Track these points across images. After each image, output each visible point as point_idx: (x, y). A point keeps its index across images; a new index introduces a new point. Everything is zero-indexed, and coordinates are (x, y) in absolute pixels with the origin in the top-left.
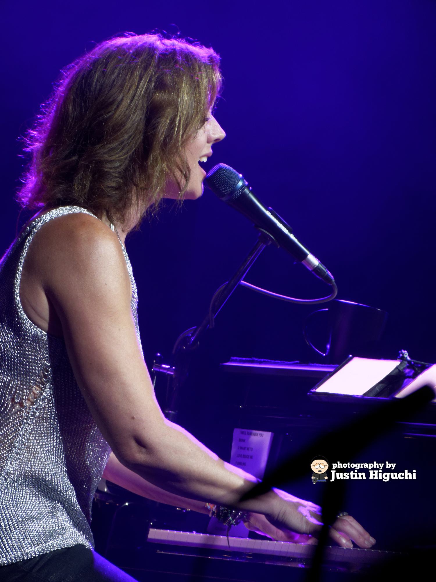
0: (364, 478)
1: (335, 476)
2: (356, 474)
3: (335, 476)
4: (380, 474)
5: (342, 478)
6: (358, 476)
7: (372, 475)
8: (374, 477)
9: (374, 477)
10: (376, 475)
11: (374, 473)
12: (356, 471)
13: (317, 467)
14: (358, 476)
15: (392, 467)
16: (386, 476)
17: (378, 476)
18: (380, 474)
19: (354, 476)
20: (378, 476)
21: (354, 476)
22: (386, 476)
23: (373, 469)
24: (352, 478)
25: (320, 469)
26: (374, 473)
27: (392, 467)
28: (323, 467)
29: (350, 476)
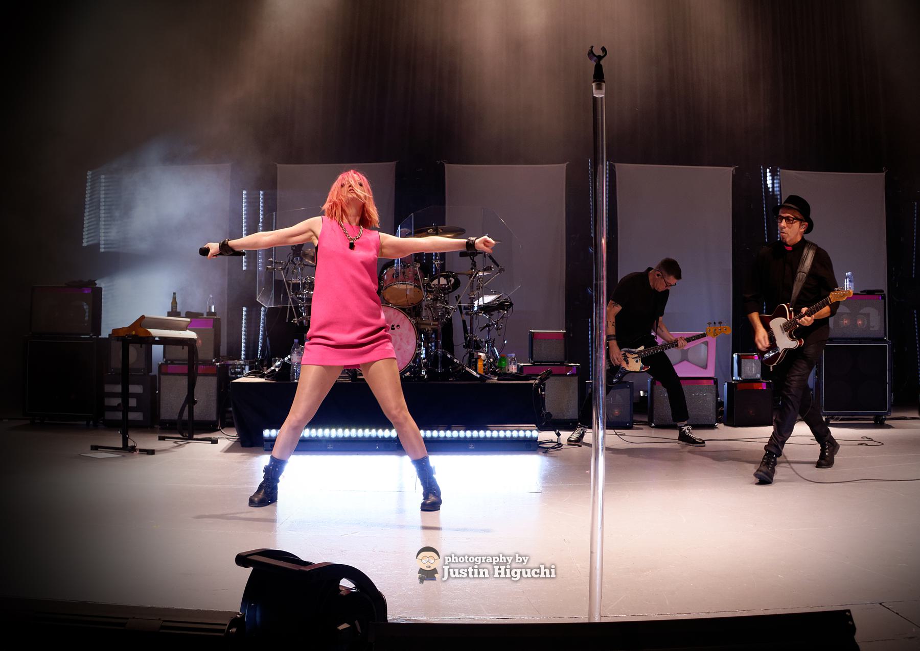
0: (487, 575)
1: (449, 573)
2: (476, 571)
3: (449, 573)
4: (508, 571)
5: (457, 575)
6: (479, 573)
7: (497, 572)
8: (500, 574)
9: (500, 574)
10: (502, 572)
11: (500, 569)
12: (476, 567)
13: (424, 561)
14: (479, 573)
15: (523, 561)
16: (516, 573)
17: (506, 574)
18: (508, 571)
19: (473, 573)
20: (506, 574)
21: (473, 573)
22: (516, 573)
23: (497, 564)
24: (471, 575)
25: (428, 564)
26: (500, 569)
27: (523, 561)
28: (432, 561)
29: (468, 573)
